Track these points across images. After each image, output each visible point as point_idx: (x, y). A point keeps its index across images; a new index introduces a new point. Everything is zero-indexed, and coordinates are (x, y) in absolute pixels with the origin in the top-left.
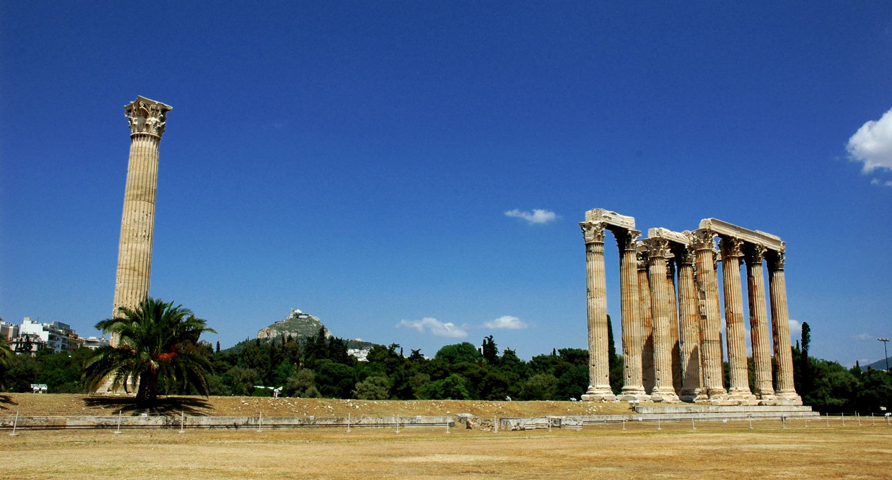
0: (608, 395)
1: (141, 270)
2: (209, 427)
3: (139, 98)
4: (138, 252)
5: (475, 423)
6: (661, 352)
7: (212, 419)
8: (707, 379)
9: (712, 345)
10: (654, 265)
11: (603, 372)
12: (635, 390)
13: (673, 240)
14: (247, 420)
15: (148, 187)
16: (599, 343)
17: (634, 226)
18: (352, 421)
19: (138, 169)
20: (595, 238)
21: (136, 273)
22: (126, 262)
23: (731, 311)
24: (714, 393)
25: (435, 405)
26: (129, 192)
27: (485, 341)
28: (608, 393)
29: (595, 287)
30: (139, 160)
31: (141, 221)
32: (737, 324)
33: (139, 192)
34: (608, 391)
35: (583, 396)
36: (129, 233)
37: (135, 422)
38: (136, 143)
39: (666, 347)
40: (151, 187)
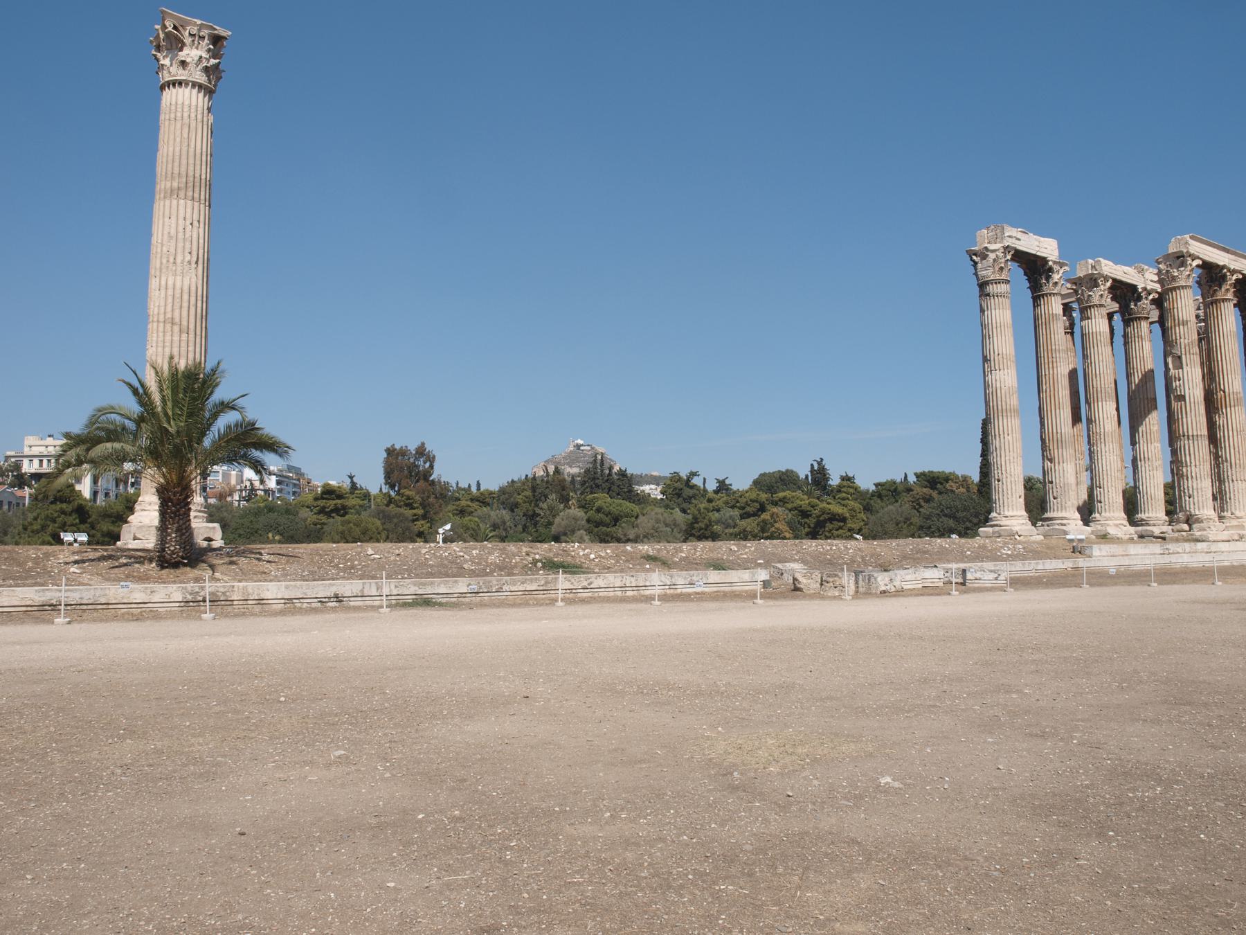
0: (1024, 527)
1: (185, 323)
2: (283, 601)
3: (163, 12)
4: (178, 292)
5: (809, 581)
6: (1104, 457)
7: (287, 587)
8: (1187, 498)
9: (1196, 443)
10: (1088, 318)
11: (1014, 491)
12: (1066, 519)
13: (1118, 278)
14: (361, 588)
15: (191, 173)
16: (1007, 444)
17: (1056, 252)
18: (575, 583)
19: (171, 142)
20: (994, 273)
21: (176, 328)
22: (159, 309)
23: (1222, 388)
24: (1199, 521)
25: (736, 549)
26: (162, 185)
27: (812, 465)
28: (1023, 524)
29: (996, 353)
30: (172, 128)
31: (181, 235)
32: (1233, 409)
33: (175, 185)
34: (1024, 521)
35: (981, 529)
36: (161, 257)
37: (123, 598)
38: (169, 96)
39: (1111, 450)
40: (197, 175)
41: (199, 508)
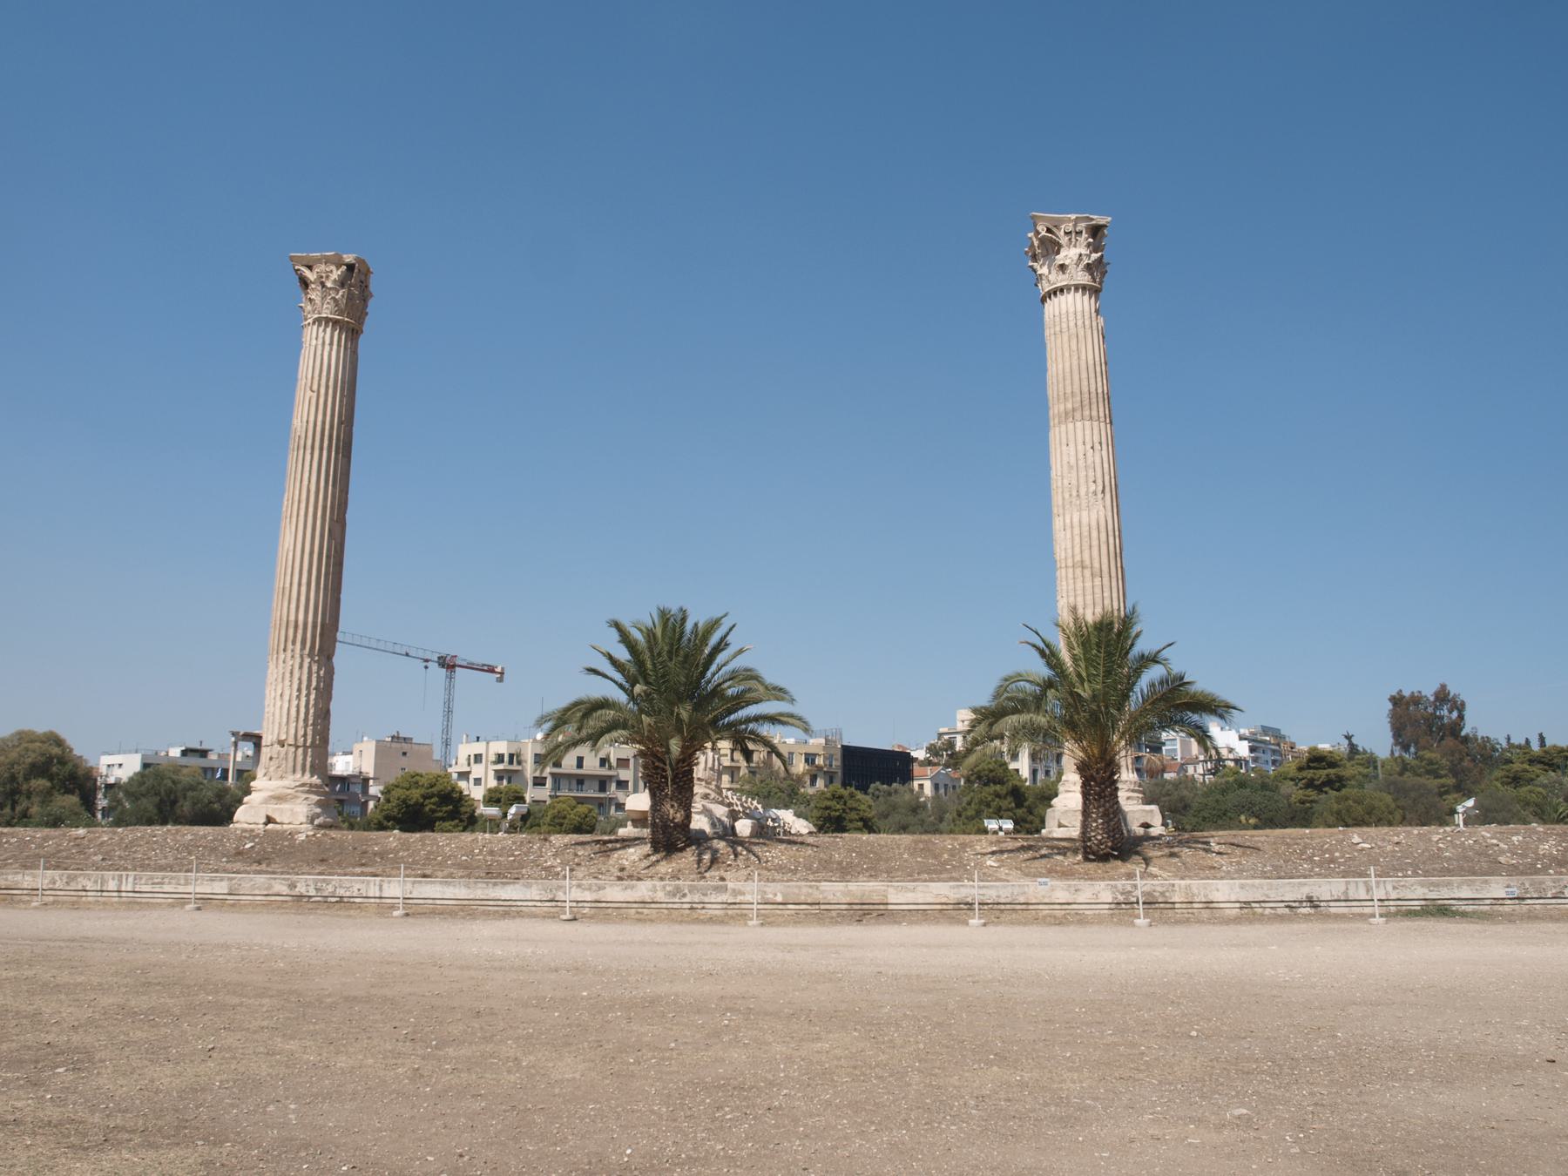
1: (1096, 565)
2: (1238, 905)
3: (1033, 217)
4: (1085, 529)
7: (1242, 887)
14: (1344, 888)
15: (1085, 390)
19: (1060, 360)
21: (1087, 573)
22: (1066, 553)
26: (1056, 409)
30: (1059, 341)
31: (1081, 463)
33: (1069, 406)
36: (1063, 492)
37: (1043, 897)
38: (1052, 307)
40: (1093, 389)
41: (1132, 787)
